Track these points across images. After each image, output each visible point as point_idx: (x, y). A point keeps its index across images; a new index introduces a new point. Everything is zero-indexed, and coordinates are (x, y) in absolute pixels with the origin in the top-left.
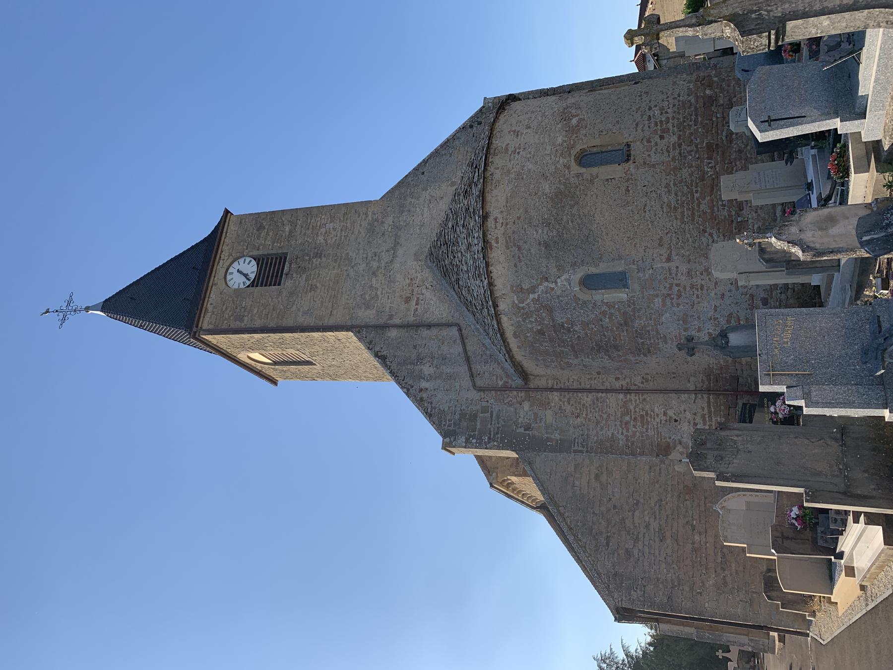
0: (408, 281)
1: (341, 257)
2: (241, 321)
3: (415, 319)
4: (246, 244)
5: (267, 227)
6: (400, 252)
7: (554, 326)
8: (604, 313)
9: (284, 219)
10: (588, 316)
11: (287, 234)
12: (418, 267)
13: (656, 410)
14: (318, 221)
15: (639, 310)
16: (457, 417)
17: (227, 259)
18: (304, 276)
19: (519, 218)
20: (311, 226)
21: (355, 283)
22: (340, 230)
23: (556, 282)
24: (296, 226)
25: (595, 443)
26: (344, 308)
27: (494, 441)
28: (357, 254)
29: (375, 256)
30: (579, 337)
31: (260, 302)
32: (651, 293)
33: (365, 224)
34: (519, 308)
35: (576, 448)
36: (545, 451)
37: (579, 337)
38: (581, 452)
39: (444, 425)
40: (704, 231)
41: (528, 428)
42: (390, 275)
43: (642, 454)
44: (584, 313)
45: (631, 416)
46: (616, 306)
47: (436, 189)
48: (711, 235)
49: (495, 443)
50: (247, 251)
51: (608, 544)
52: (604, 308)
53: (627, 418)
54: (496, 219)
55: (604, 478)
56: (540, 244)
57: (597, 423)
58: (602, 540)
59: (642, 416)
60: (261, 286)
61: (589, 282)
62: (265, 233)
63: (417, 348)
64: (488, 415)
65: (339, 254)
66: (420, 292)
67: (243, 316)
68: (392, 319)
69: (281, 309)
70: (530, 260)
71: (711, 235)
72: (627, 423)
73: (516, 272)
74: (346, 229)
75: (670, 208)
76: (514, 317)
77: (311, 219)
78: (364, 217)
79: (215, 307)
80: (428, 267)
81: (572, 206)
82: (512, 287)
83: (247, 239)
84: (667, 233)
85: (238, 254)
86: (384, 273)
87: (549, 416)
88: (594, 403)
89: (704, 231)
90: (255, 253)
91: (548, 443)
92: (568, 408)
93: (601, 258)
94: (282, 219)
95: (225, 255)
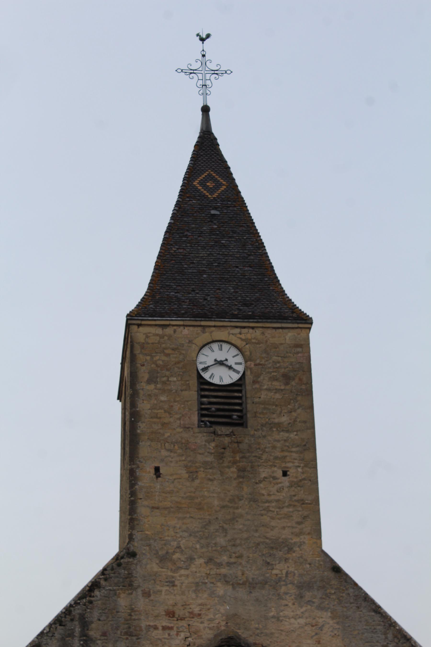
0: (196, 610)
1: (237, 508)
3: (143, 628)
4: (263, 362)
5: (288, 387)
6: (242, 593)
9: (299, 411)
11: (276, 421)
12: (217, 621)
14: (293, 463)
17: (240, 338)
18: (210, 459)
21: (197, 534)
22: (277, 498)
26: (162, 525)
28: (240, 530)
29: (237, 557)
31: (175, 401)
42: (206, 583)
47: (332, 631)
50: (252, 366)
62: (279, 387)
63: (103, 638)
65: (241, 502)
66: (181, 629)
67: (156, 383)
68: (143, 596)
69: (163, 435)
74: (279, 508)
77: (296, 452)
78: (297, 530)
79: (170, 337)
80: (216, 636)
83: (271, 361)
85: (248, 353)
86: (211, 573)
94: (298, 408)
95: (249, 334)
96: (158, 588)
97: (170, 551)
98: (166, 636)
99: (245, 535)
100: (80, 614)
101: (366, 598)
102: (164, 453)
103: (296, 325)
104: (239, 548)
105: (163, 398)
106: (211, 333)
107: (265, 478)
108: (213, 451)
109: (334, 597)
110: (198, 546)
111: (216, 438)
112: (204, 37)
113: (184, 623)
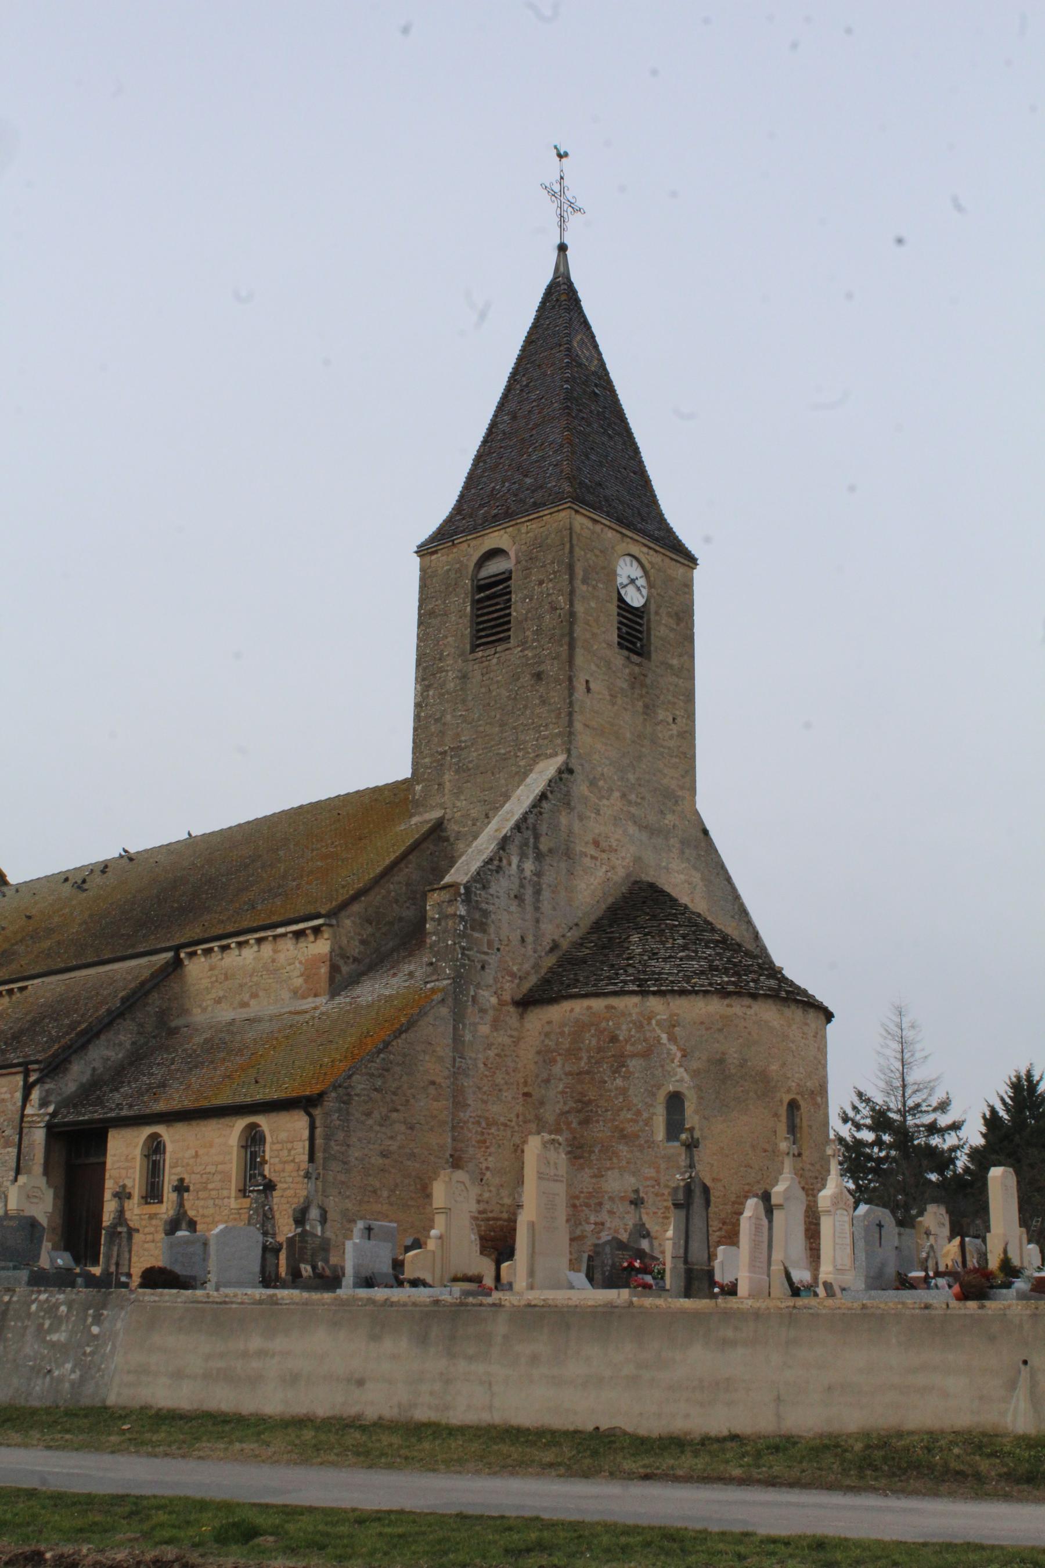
2: (585, 581)
3: (578, 853)
5: (678, 628)
6: (644, 836)
7: (622, 1056)
8: (638, 1113)
10: (636, 1096)
13: (490, 1159)
16: (484, 906)
19: (749, 1033)
20: (676, 700)
23: (681, 1066)
24: (677, 676)
25: (462, 1084)
27: (463, 954)
30: (606, 1082)
32: (662, 1166)
34: (650, 1019)
35: (458, 1060)
36: (454, 1020)
37: (606, 1082)
38: (454, 1067)
39: (476, 887)
40: (724, 1223)
41: (474, 998)
43: (454, 1139)
44: (640, 1092)
45: (484, 1128)
46: (647, 1128)
48: (720, 1229)
49: (460, 956)
51: (376, 1090)
52: (645, 1115)
53: (484, 1124)
54: (750, 1007)
55: (432, 1090)
56: (723, 1054)
57: (480, 1088)
58: (379, 1083)
59: (484, 1142)
60: (619, 614)
61: (675, 1101)
64: (486, 950)
67: (588, 584)
70: (706, 1041)
71: (720, 1229)
72: (479, 1123)
73: (695, 1023)
75: (747, 1192)
76: (637, 1010)
81: (756, 1093)
82: (677, 1015)
84: (724, 1187)
85: (652, 579)
87: (484, 1029)
88: (497, 1085)
89: (724, 1223)
90: (653, 607)
91: (461, 1025)
92: (491, 1053)
93: (705, 1118)
95: (657, 559)
96: (588, 814)
97: (598, 777)
98: (593, 866)
100: (533, 823)
101: (723, 867)
102: (593, 667)
103: (686, 562)
105: (593, 604)
106: (628, 543)
107: (662, 721)
108: (627, 678)
109: (703, 859)
110: (616, 778)
111: (630, 665)
112: (562, 153)
113: (605, 856)
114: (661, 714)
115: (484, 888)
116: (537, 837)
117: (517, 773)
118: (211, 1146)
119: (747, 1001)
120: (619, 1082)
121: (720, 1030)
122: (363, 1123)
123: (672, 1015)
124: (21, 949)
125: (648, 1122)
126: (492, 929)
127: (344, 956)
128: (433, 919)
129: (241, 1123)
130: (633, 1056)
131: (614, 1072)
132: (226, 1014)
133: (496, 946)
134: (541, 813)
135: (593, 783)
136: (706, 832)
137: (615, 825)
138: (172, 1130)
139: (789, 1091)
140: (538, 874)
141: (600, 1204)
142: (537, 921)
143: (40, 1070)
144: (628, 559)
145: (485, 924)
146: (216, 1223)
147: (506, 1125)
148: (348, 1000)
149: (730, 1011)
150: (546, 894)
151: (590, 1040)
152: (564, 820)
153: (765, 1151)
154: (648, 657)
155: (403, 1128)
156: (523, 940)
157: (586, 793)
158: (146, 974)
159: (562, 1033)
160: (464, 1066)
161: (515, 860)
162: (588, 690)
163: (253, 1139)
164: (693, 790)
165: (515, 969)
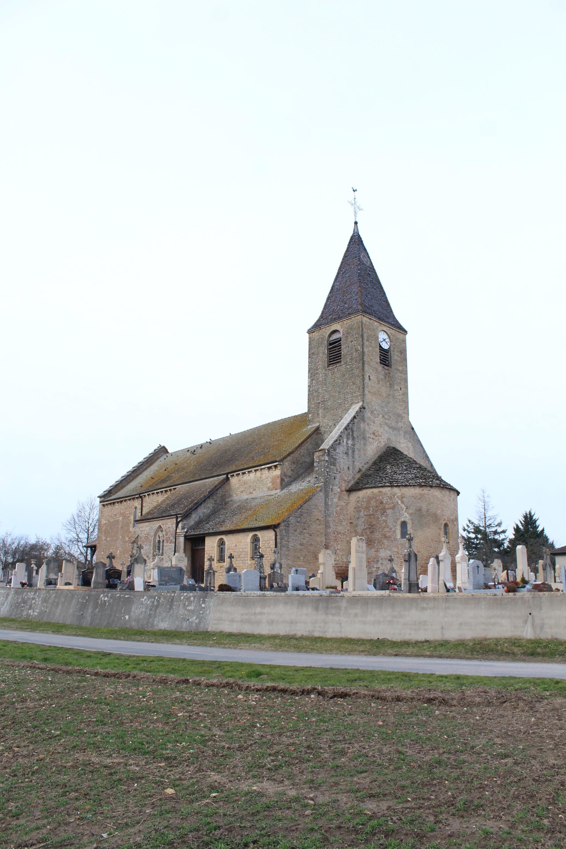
2: (367, 340)
6: (391, 431)
7: (385, 509)
8: (391, 529)
13: (339, 546)
15: (392, 542)
16: (334, 457)
23: (406, 512)
24: (401, 373)
27: (327, 474)
33: (401, 412)
34: (394, 495)
40: (422, 567)
43: (326, 539)
48: (421, 569)
51: (298, 522)
52: (393, 529)
53: (336, 534)
54: (430, 490)
55: (317, 522)
56: (421, 507)
57: (334, 521)
60: (380, 352)
61: (404, 524)
71: (421, 569)
72: (334, 533)
76: (390, 492)
81: (433, 521)
87: (336, 500)
89: (422, 567)
90: (392, 349)
95: (393, 332)
99: (391, 409)
101: (419, 441)
102: (371, 371)
104: (390, 414)
105: (370, 349)
113: (377, 438)
114: (396, 387)
115: (334, 450)
116: (353, 432)
117: (345, 409)
118: (241, 542)
119: (429, 488)
120: (384, 518)
121: (419, 499)
122: (294, 534)
123: (402, 494)
124: (174, 475)
125: (394, 532)
126: (337, 465)
127: (285, 475)
128: (316, 462)
129: (251, 534)
130: (389, 509)
131: (382, 515)
132: (245, 496)
133: (339, 470)
134: (354, 423)
135: (372, 412)
136: (413, 429)
137: (380, 427)
138: (227, 537)
139: (444, 520)
140: (353, 445)
141: (378, 561)
142: (354, 462)
143: (182, 517)
144: (383, 332)
145: (335, 463)
146: (243, 569)
147: (344, 534)
148: (287, 491)
149: (423, 492)
150: (356, 452)
151: (373, 503)
152: (362, 425)
153: (436, 541)
154: (391, 367)
155: (307, 535)
156: (348, 468)
157: (370, 416)
158: (217, 483)
159: (363, 501)
160: (329, 513)
161: (345, 440)
162: (370, 379)
163: (256, 540)
164: (408, 414)
165: (346, 479)
